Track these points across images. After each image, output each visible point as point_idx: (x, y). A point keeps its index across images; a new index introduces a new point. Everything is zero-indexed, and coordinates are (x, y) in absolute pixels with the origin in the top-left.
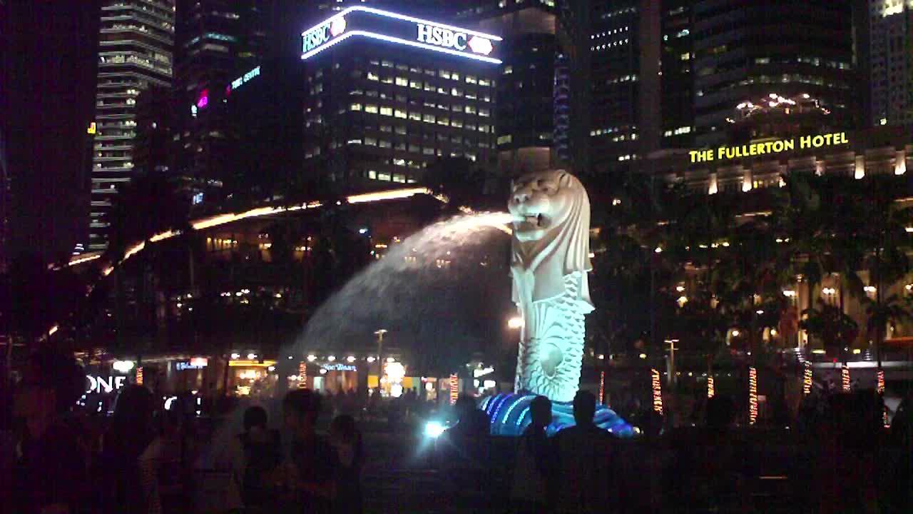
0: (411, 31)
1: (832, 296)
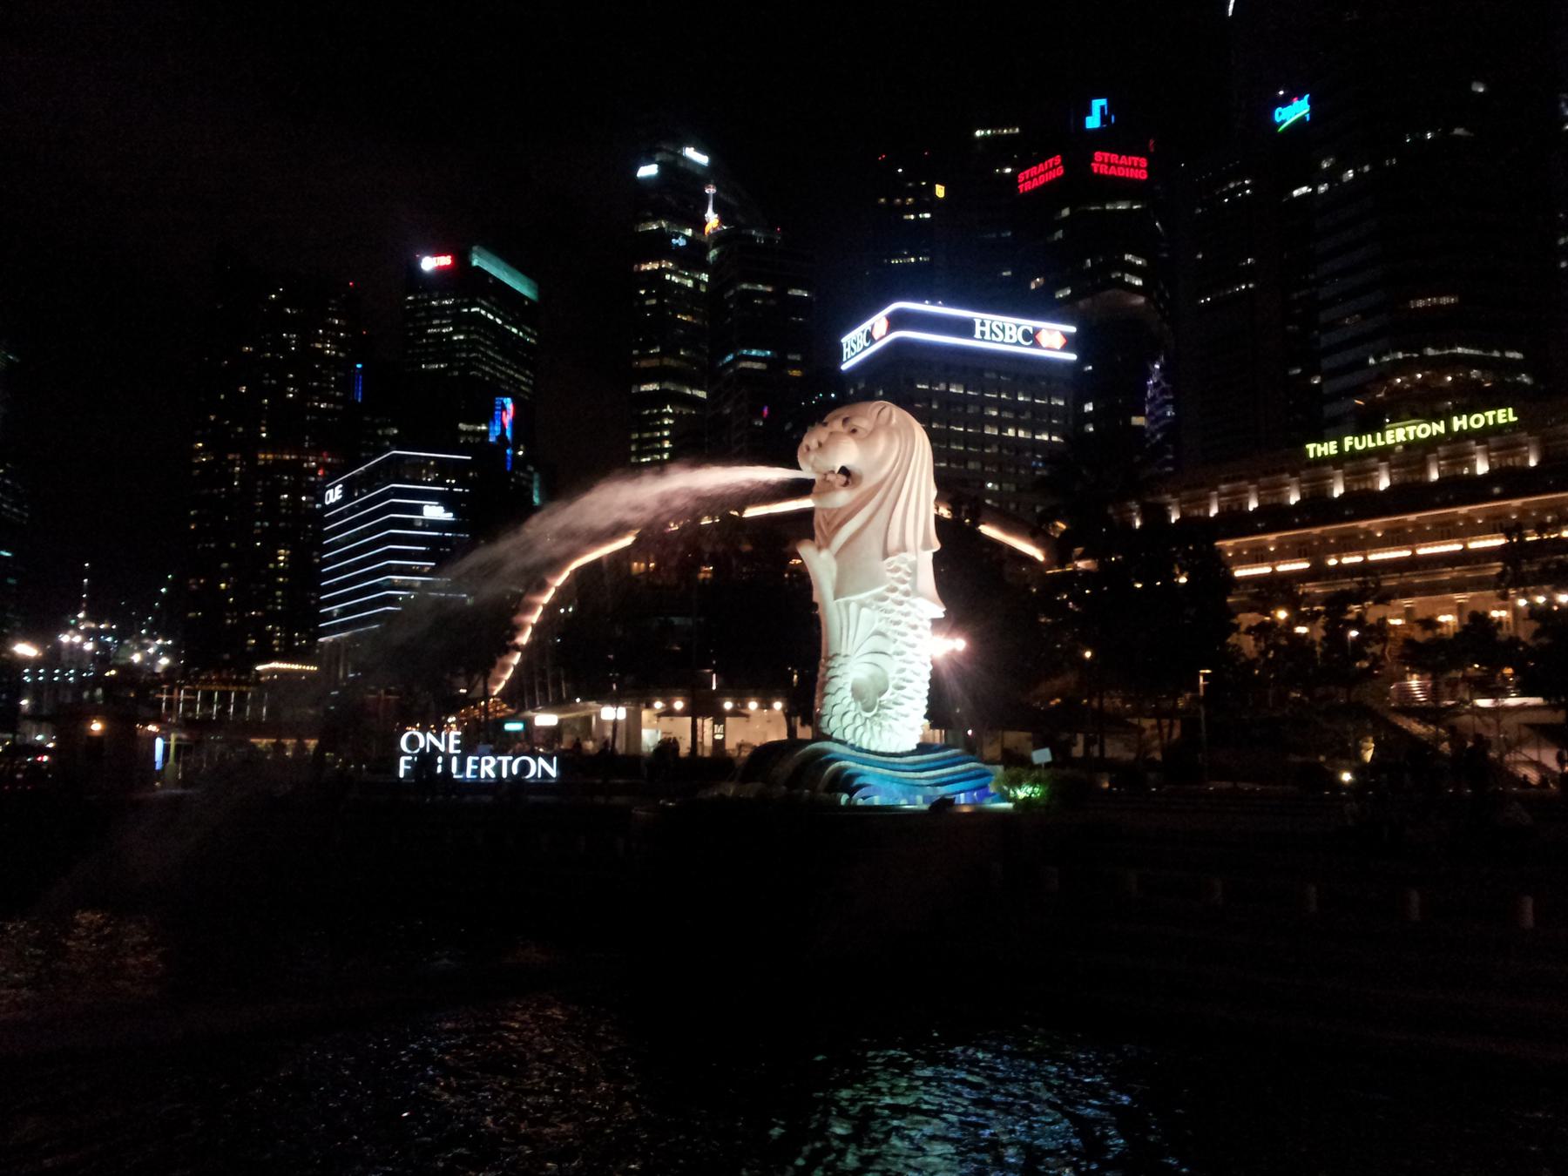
0: (966, 328)
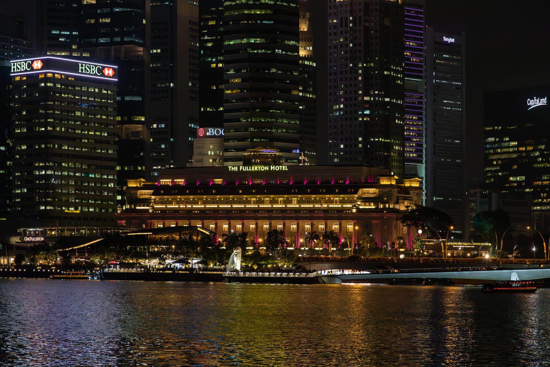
0: (74, 68)
1: (281, 228)
